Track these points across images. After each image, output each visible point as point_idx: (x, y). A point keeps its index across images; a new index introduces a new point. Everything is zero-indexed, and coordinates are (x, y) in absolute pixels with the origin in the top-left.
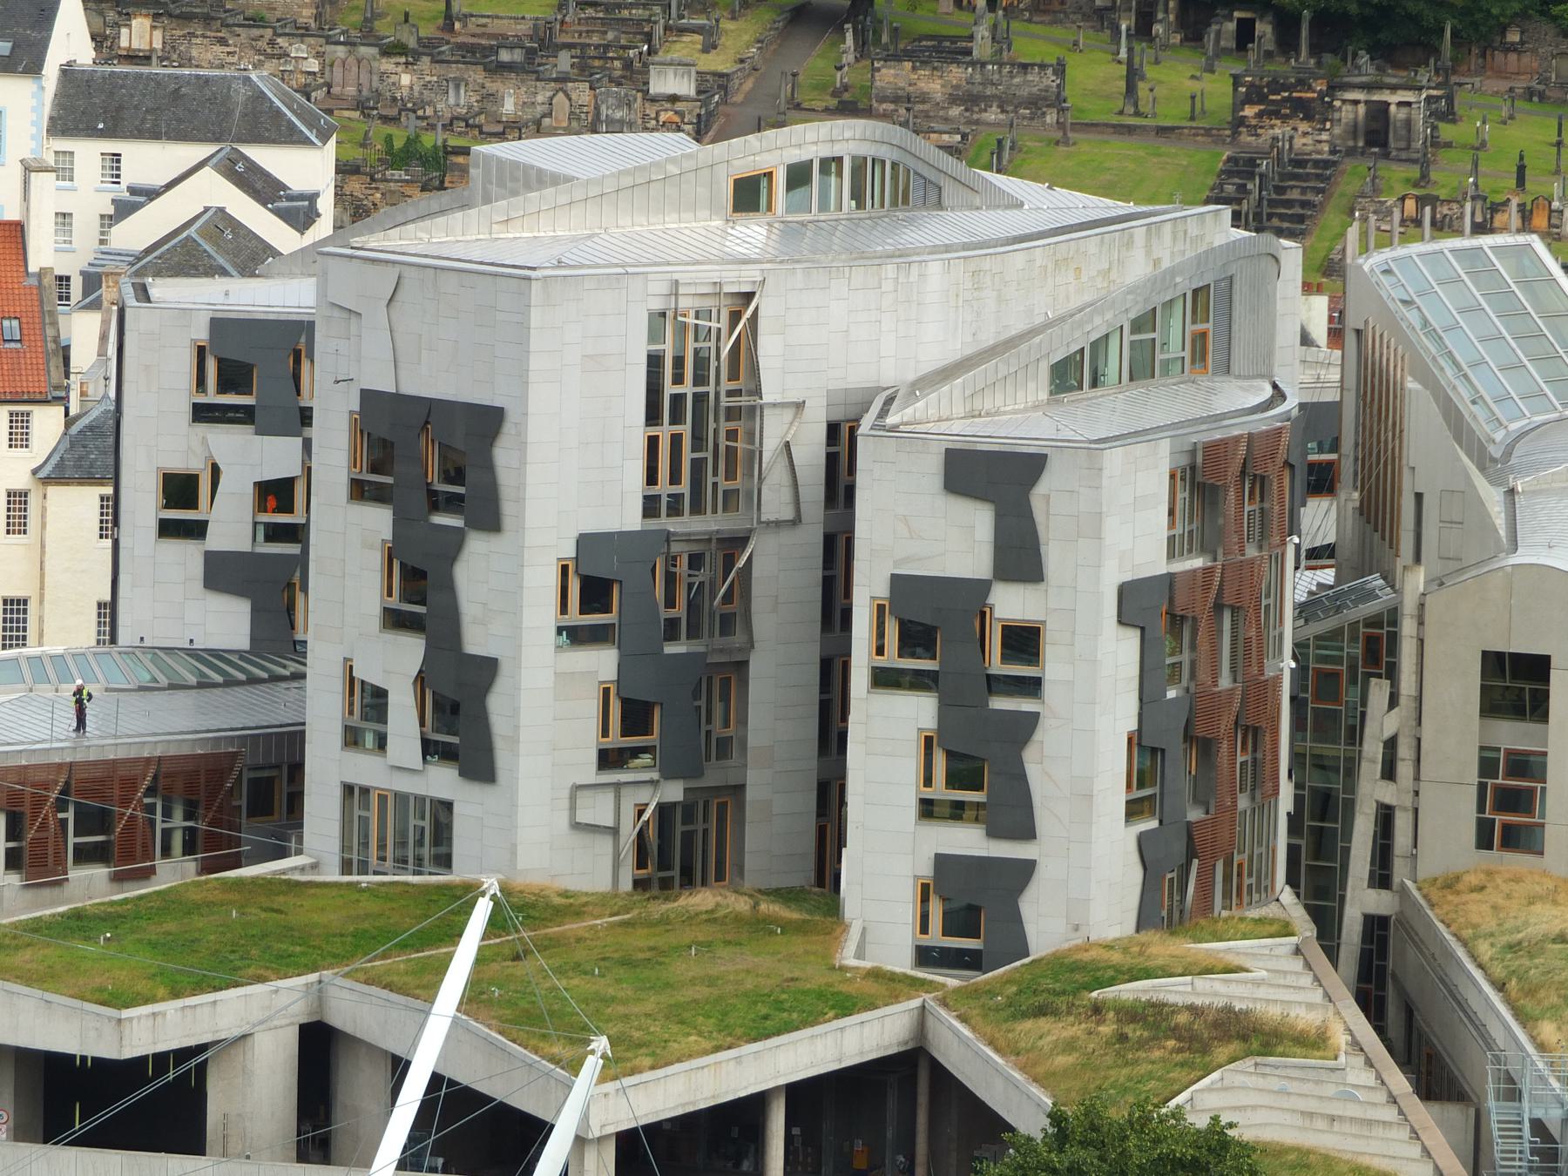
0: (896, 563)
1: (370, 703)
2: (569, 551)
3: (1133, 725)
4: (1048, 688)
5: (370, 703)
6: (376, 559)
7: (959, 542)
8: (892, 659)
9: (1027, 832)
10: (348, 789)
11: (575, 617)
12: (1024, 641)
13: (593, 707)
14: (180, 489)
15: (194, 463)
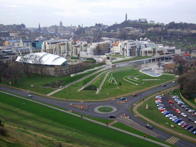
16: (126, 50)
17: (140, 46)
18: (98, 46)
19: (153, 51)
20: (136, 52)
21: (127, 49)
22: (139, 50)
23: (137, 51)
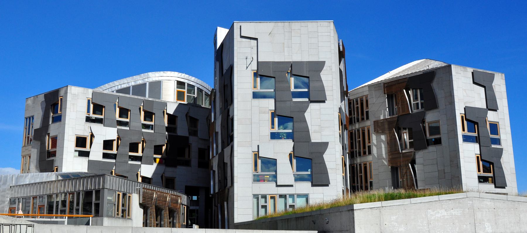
0: (465, 103)
1: (267, 166)
4: (502, 142)
5: (267, 166)
6: (269, 117)
8: (466, 133)
10: (256, 196)
14: (81, 142)
15: (87, 134)
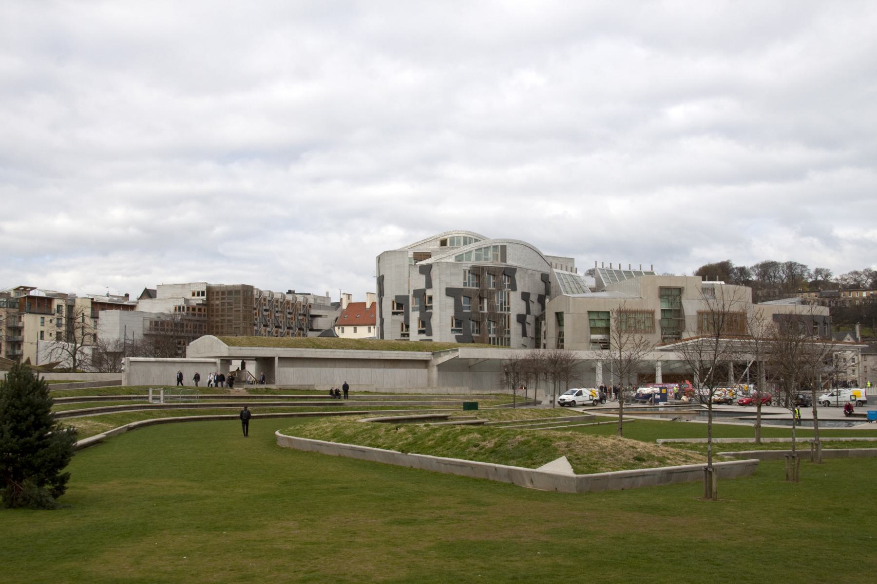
2: (394, 298)
3: (453, 314)
7: (419, 282)
9: (430, 334)
11: (395, 310)
12: (430, 298)
13: (400, 326)
16: (424, 301)
17: (545, 278)
18: (207, 304)
19: (658, 316)
20: (515, 327)
21: (437, 293)
22: (535, 308)
23: (521, 319)
